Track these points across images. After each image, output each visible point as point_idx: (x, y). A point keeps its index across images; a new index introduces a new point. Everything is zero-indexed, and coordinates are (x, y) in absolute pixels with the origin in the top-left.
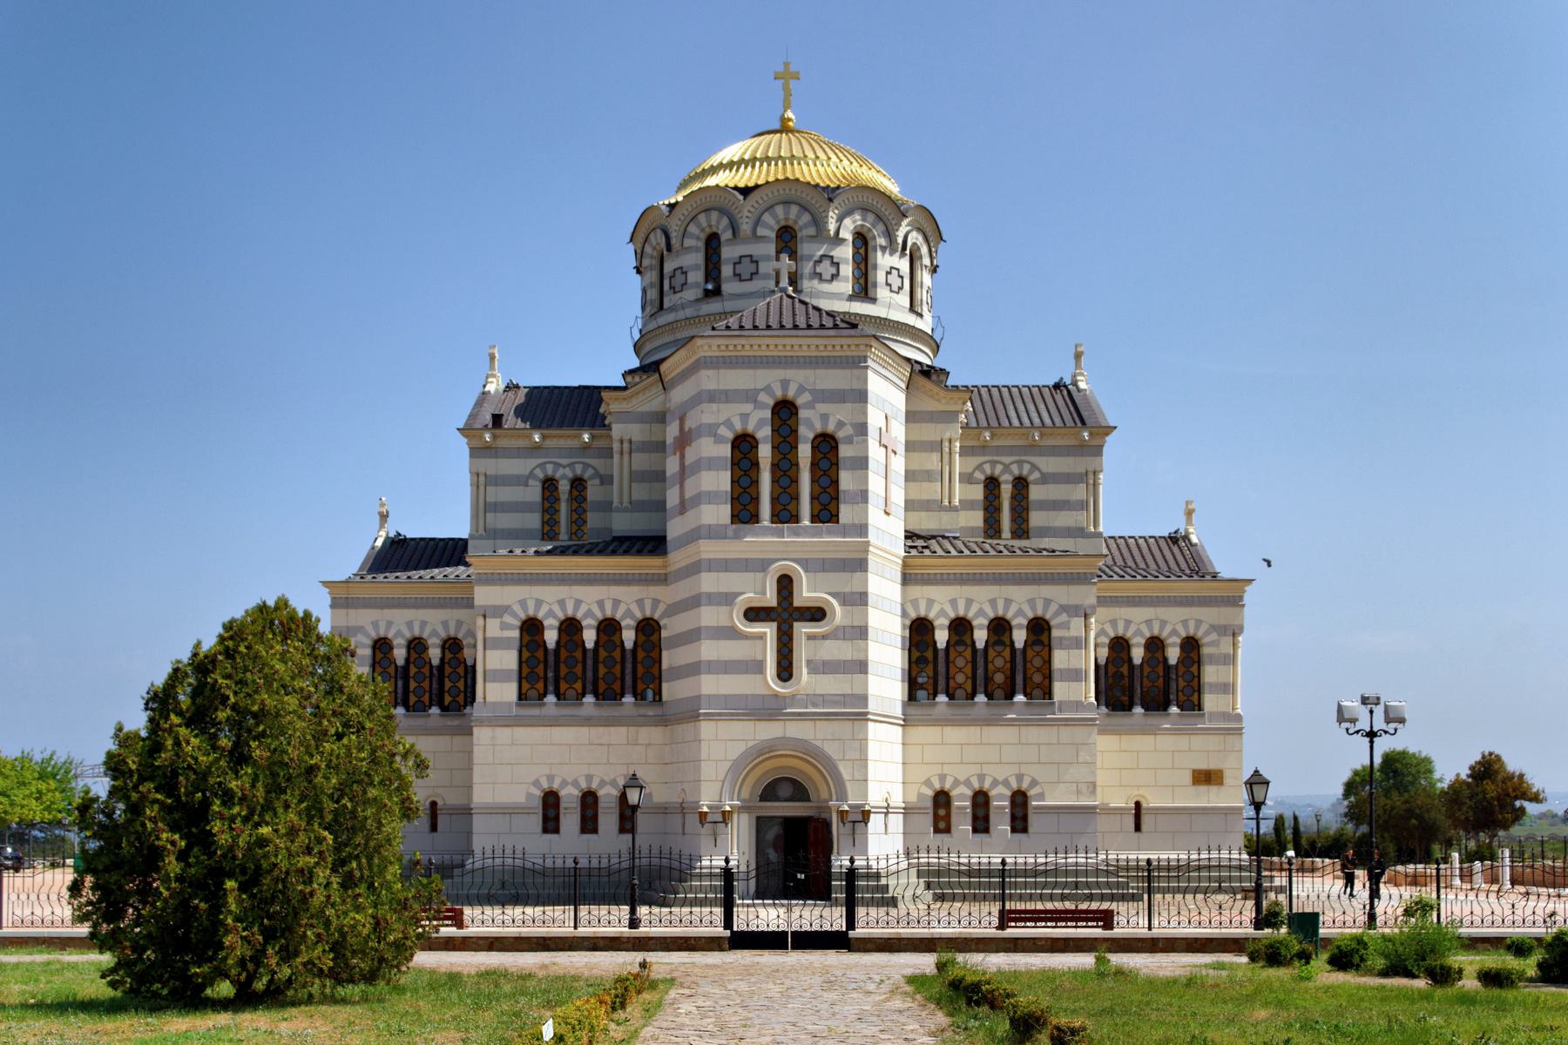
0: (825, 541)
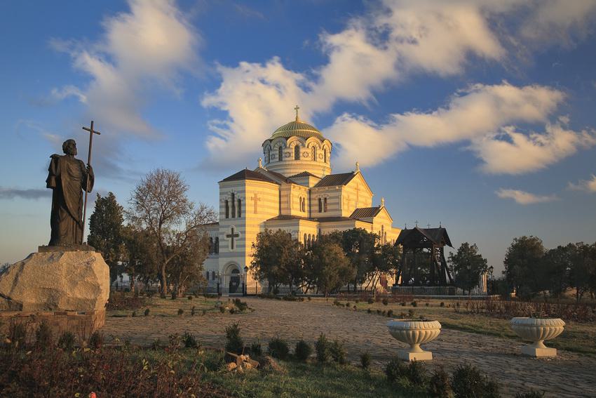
0: (238, 222)
